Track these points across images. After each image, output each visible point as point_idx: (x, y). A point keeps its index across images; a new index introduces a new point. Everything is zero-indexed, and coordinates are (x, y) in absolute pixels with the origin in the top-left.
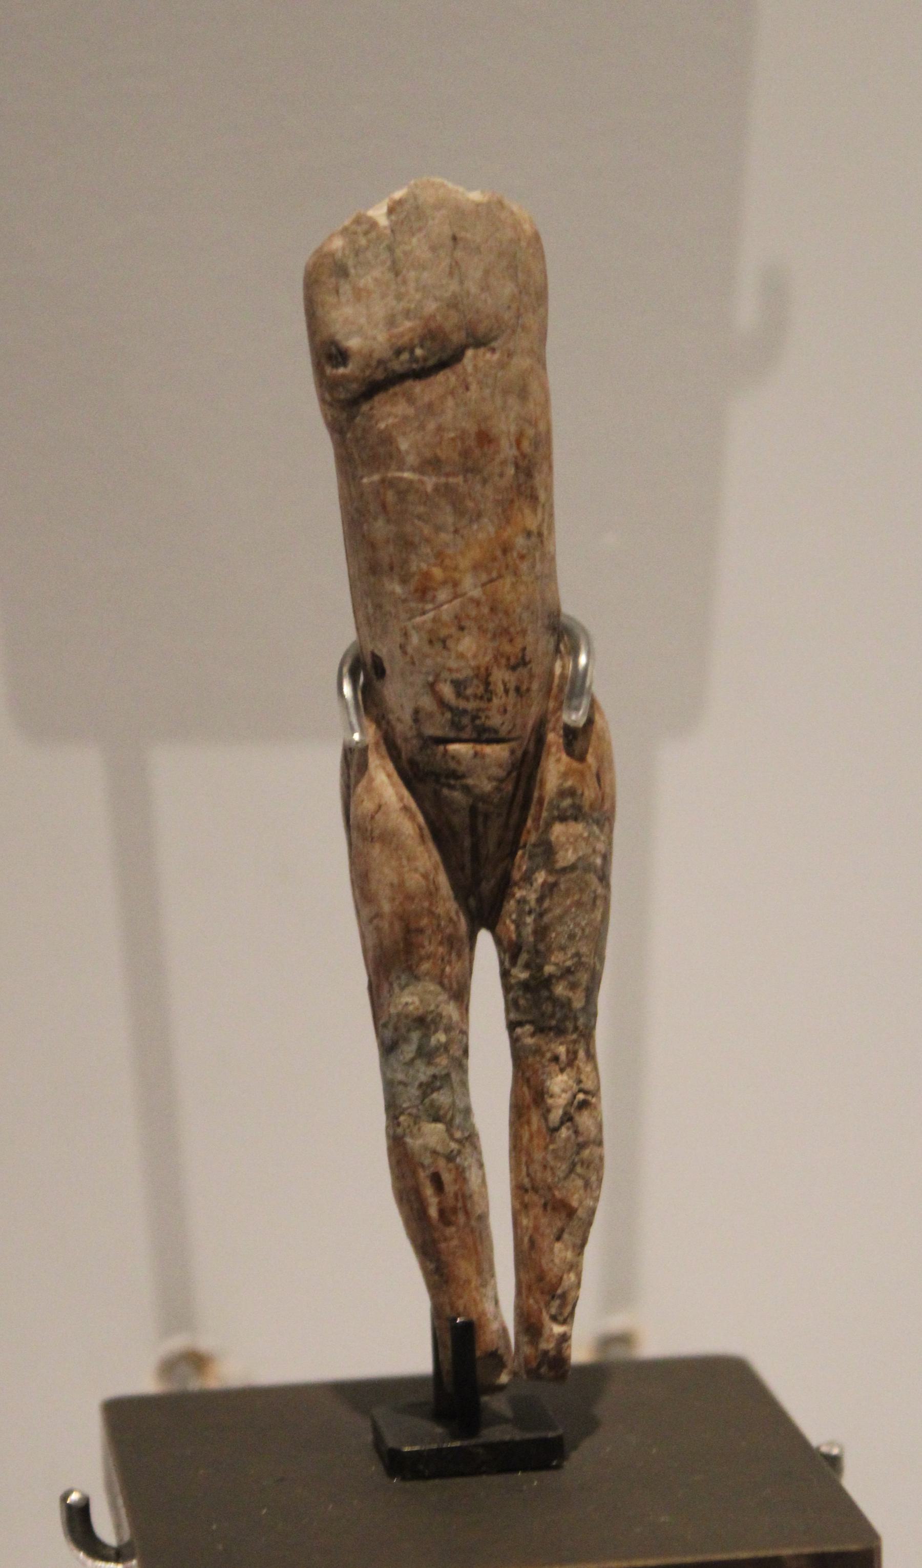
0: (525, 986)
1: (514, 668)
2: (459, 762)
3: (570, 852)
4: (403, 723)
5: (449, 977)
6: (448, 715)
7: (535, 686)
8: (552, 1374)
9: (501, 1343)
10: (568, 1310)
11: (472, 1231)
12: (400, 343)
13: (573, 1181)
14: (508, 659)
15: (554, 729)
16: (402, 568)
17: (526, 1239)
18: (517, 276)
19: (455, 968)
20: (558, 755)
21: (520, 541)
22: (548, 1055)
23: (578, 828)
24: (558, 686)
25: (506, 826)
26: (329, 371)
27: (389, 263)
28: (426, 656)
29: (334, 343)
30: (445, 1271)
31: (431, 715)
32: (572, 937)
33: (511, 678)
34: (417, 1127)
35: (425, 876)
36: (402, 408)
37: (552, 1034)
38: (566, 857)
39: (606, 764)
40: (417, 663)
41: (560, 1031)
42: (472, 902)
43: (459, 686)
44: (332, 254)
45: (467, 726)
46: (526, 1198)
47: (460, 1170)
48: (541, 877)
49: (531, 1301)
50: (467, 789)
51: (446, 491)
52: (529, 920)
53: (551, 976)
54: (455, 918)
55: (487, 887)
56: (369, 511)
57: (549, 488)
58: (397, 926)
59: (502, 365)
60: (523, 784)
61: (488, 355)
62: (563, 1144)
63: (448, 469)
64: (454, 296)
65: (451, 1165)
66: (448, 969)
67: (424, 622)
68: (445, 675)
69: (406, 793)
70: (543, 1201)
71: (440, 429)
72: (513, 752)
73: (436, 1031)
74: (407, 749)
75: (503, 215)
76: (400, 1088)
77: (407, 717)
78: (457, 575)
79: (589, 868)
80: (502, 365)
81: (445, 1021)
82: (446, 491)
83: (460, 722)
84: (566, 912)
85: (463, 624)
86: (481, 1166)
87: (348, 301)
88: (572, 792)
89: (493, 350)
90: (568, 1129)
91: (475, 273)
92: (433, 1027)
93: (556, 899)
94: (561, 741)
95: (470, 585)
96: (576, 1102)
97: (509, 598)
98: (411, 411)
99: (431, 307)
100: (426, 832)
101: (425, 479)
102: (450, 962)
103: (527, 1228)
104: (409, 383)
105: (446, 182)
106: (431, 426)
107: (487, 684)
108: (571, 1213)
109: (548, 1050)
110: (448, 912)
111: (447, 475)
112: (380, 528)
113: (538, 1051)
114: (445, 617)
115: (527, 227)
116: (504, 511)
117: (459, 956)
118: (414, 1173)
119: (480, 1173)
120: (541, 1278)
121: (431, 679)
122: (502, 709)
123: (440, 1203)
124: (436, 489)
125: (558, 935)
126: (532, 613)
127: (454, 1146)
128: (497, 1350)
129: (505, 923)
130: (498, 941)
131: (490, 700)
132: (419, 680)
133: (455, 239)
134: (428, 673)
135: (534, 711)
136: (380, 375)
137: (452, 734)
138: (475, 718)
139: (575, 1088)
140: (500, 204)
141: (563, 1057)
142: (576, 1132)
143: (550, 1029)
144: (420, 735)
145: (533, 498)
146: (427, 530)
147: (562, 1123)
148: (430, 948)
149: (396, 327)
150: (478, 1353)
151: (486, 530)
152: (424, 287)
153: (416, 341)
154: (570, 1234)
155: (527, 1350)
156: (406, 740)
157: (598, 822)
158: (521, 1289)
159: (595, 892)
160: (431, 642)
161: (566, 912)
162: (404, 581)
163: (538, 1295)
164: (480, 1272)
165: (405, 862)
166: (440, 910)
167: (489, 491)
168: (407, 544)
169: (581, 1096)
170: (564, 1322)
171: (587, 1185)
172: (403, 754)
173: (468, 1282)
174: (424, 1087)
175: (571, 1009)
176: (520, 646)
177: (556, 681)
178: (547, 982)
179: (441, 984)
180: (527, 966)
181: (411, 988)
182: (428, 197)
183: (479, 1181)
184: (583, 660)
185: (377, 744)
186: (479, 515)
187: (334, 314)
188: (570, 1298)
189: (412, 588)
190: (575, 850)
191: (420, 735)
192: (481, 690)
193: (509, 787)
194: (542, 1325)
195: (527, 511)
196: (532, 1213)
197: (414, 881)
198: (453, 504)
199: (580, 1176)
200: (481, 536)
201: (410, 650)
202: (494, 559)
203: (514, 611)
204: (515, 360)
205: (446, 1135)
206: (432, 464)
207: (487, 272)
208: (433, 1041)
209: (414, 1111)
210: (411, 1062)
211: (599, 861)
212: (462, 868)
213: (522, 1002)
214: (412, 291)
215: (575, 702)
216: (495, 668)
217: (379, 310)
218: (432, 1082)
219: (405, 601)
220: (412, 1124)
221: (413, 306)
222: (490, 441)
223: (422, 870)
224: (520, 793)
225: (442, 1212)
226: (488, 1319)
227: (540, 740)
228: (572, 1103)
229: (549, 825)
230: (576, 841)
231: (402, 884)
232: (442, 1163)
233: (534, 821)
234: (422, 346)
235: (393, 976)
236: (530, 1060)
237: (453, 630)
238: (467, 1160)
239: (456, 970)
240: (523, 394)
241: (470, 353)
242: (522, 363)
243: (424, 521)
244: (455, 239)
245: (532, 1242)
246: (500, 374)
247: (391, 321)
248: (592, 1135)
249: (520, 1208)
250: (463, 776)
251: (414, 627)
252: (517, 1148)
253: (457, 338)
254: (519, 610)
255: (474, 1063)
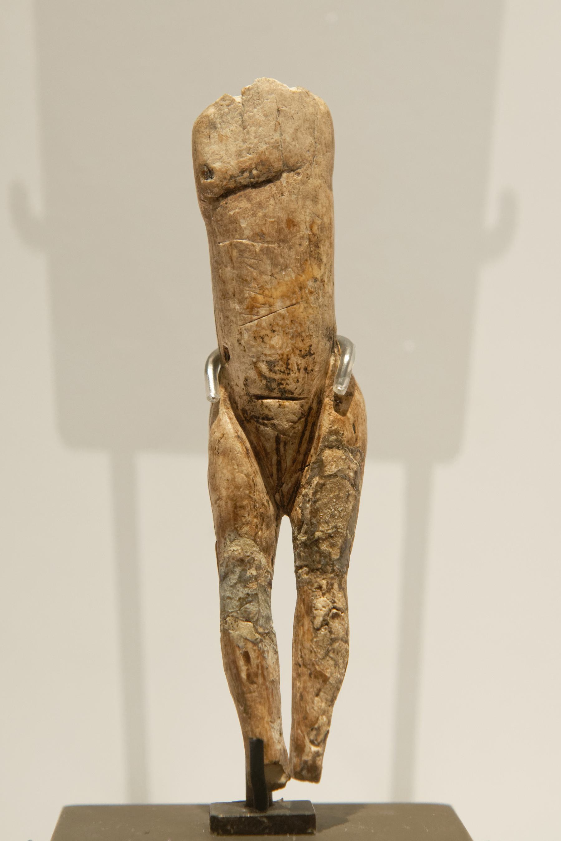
0: (305, 544)
1: (304, 357)
2: (270, 410)
3: (334, 467)
4: (239, 389)
5: (261, 538)
6: (264, 382)
7: (317, 368)
8: (310, 775)
9: (282, 758)
10: (321, 737)
11: (267, 688)
12: (243, 166)
13: (328, 661)
14: (301, 351)
15: (328, 396)
16: (240, 294)
17: (298, 695)
18: (314, 133)
19: (264, 533)
20: (330, 411)
21: (310, 284)
22: (316, 585)
23: (339, 453)
24: (332, 371)
25: (298, 452)
26: (202, 181)
27: (240, 122)
28: (253, 346)
29: (206, 165)
30: (250, 711)
31: (254, 381)
32: (333, 516)
33: (302, 363)
34: (236, 623)
35: (247, 476)
36: (244, 204)
37: (318, 573)
38: (331, 469)
39: (360, 420)
40: (247, 351)
41: (324, 572)
42: (277, 496)
43: (271, 365)
44: (207, 116)
45: (275, 389)
46: (300, 671)
47: (262, 651)
48: (316, 480)
49: (299, 731)
50: (274, 426)
51: (267, 252)
52: (308, 505)
53: (319, 538)
54: (266, 504)
55: (286, 488)
56: (222, 262)
57: (330, 256)
58: (230, 504)
59: (303, 183)
60: (309, 428)
61: (295, 177)
62: (322, 638)
63: (269, 239)
64: (277, 141)
65: (255, 648)
66: (260, 533)
67: (252, 326)
68: (263, 358)
69: (240, 429)
70: (309, 672)
71: (265, 216)
72: (302, 406)
73: (250, 568)
74: (241, 402)
75: (308, 100)
76: (228, 601)
77: (241, 383)
78: (271, 300)
79: (345, 477)
80: (303, 183)
81: (256, 562)
82: (267, 252)
83: (271, 386)
84: (330, 501)
85: (274, 329)
86: (276, 652)
87: (215, 142)
88: (336, 432)
89: (299, 174)
90: (326, 629)
91: (289, 129)
92: (248, 565)
93: (324, 493)
94: (332, 403)
95: (278, 306)
96: (331, 615)
97: (302, 315)
98: (249, 206)
99: (263, 147)
100: (251, 452)
101: (255, 244)
102: (262, 530)
103: (299, 688)
104: (249, 190)
105: (276, 81)
106: (260, 214)
107: (288, 364)
108: (325, 680)
109: (316, 582)
110: (262, 500)
111: (268, 242)
112: (229, 272)
113: (310, 583)
114: (264, 324)
115: (322, 107)
116: (301, 265)
117: (268, 527)
118: (234, 652)
119: (275, 657)
120: (305, 718)
121: (254, 360)
122: (296, 380)
123: (248, 670)
124: (261, 250)
125: (325, 514)
126: (316, 325)
127: (257, 636)
128: (279, 761)
129: (296, 510)
130: (292, 521)
131: (289, 374)
132: (247, 360)
133: (279, 111)
134: (253, 357)
135: (315, 384)
136: (232, 185)
137: (266, 393)
138: (280, 384)
139: (331, 605)
140: (307, 94)
141: (324, 587)
142: (330, 632)
143: (317, 570)
144: (248, 394)
145: (319, 260)
146: (255, 273)
147: (322, 626)
148: (249, 519)
149: (242, 157)
150: (266, 762)
151: (289, 276)
152: (260, 136)
153: (253, 166)
154: (325, 693)
155: (295, 760)
156: (240, 397)
157: (352, 452)
158: (296, 724)
159: (348, 491)
160: (255, 338)
161: (330, 501)
162: (241, 302)
163: (303, 728)
164: (270, 713)
165: (236, 467)
166: (256, 497)
167: (292, 253)
168: (243, 281)
169: (335, 611)
170: (318, 745)
171: (336, 665)
172: (239, 405)
173: (262, 718)
174: (241, 600)
175: (330, 560)
176: (308, 344)
177: (331, 368)
178: (317, 542)
179: (255, 541)
180: (306, 533)
181: (236, 542)
182: (264, 87)
183: (274, 661)
184: (347, 358)
185: (225, 400)
186: (287, 267)
187: (207, 149)
188: (324, 729)
189: (245, 307)
190: (337, 466)
191: (248, 394)
192: (283, 368)
193: (299, 427)
194: (305, 746)
195: (315, 267)
196: (302, 679)
197: (241, 478)
198: (271, 259)
199: (332, 658)
200: (287, 279)
201: (243, 342)
202: (294, 293)
203: (305, 324)
204: (311, 180)
205: (253, 629)
206: (260, 236)
207: (296, 130)
208: (248, 574)
209: (235, 614)
210: (234, 586)
211: (352, 474)
212: (272, 475)
213: (302, 554)
214: (252, 137)
215: (340, 380)
216: (292, 355)
217: (233, 148)
218: (247, 598)
219: (240, 314)
220: (233, 623)
221: (252, 146)
222: (294, 225)
223: (245, 472)
224: (307, 434)
225: (248, 676)
226: (274, 742)
227: (320, 402)
228: (329, 614)
229: (322, 450)
230: (338, 460)
231: (234, 479)
232: (250, 646)
233: (314, 449)
234: (257, 169)
235: (226, 536)
236: (306, 588)
237: (268, 332)
238: (266, 646)
239: (265, 535)
240: (315, 199)
241: (285, 175)
242: (315, 182)
243: (253, 268)
244: (279, 111)
245: (301, 696)
246: (301, 187)
247: (239, 154)
248: (341, 635)
249: (297, 676)
250: (272, 419)
251: (245, 329)
252: (297, 641)
253: (278, 165)
254: (308, 323)
255: (275, 591)
